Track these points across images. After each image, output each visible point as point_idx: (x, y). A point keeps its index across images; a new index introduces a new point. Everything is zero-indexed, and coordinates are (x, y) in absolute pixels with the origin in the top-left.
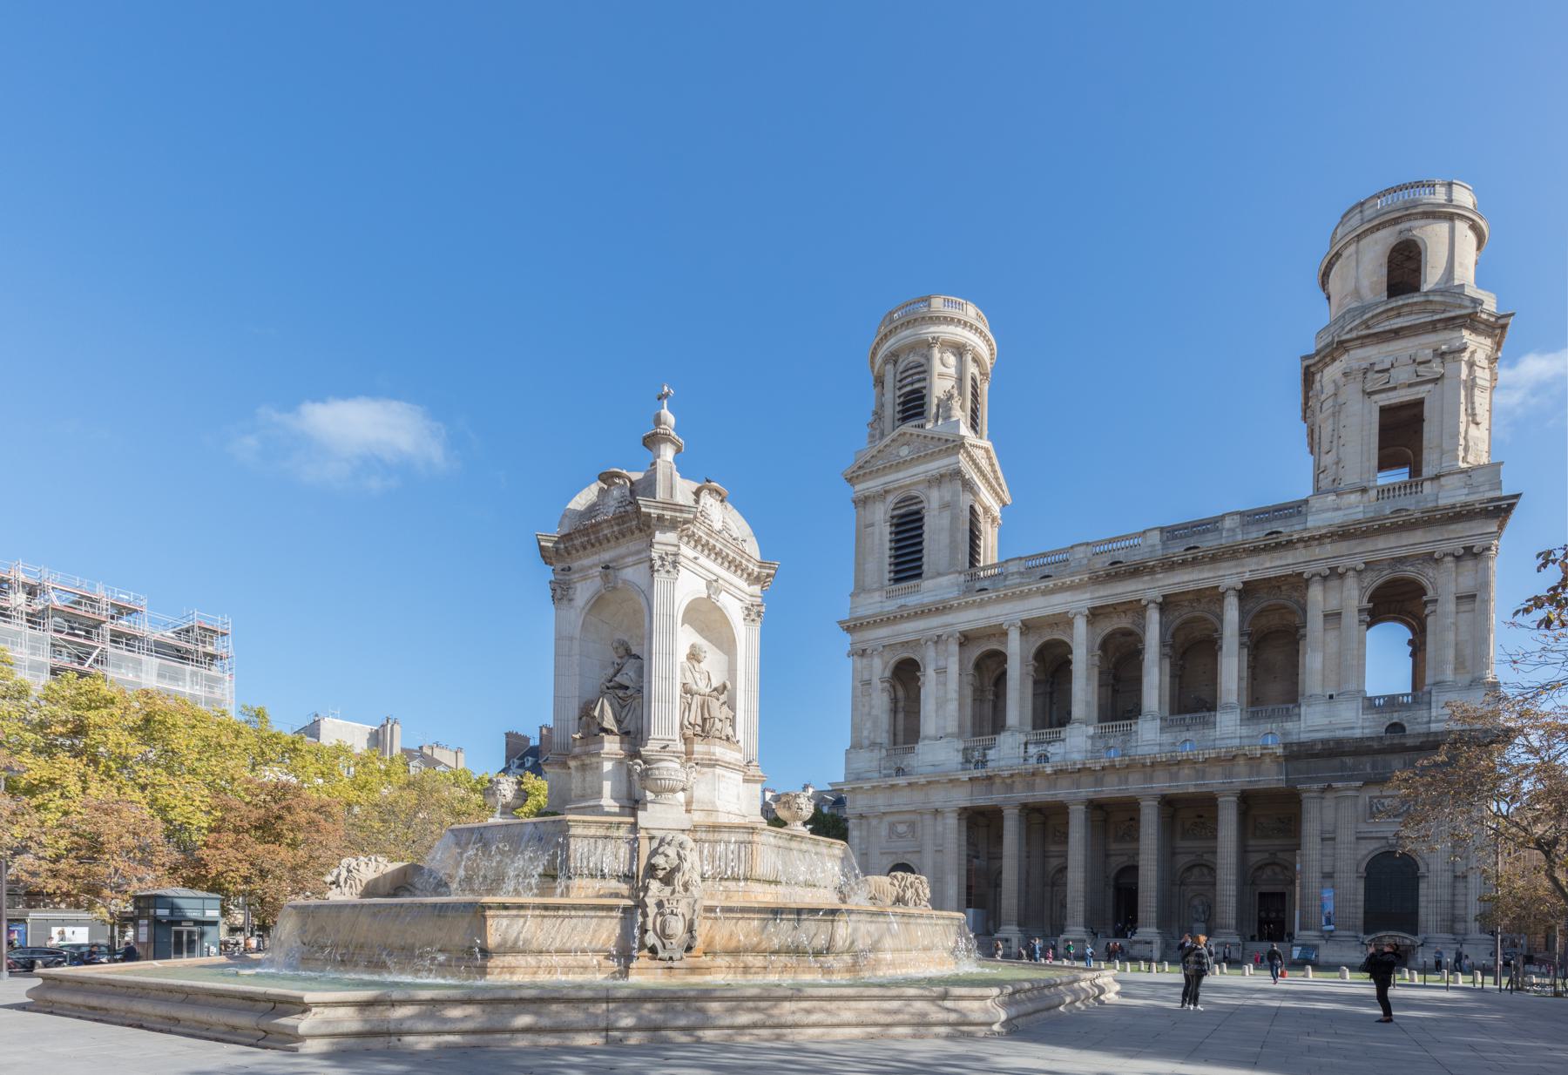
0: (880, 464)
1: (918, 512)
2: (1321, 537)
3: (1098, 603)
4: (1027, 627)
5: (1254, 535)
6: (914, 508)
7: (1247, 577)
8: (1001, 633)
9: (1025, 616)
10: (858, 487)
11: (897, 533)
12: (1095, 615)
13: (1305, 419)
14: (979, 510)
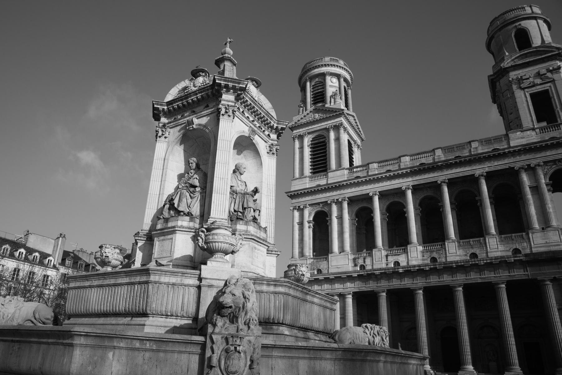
0: (304, 121)
1: (324, 142)
2: (520, 150)
3: (416, 183)
4: (383, 195)
5: (486, 150)
6: (322, 140)
7: (487, 170)
8: (368, 199)
9: (380, 190)
10: (295, 132)
11: (313, 151)
12: (416, 189)
13: (494, 101)
14: (352, 142)
